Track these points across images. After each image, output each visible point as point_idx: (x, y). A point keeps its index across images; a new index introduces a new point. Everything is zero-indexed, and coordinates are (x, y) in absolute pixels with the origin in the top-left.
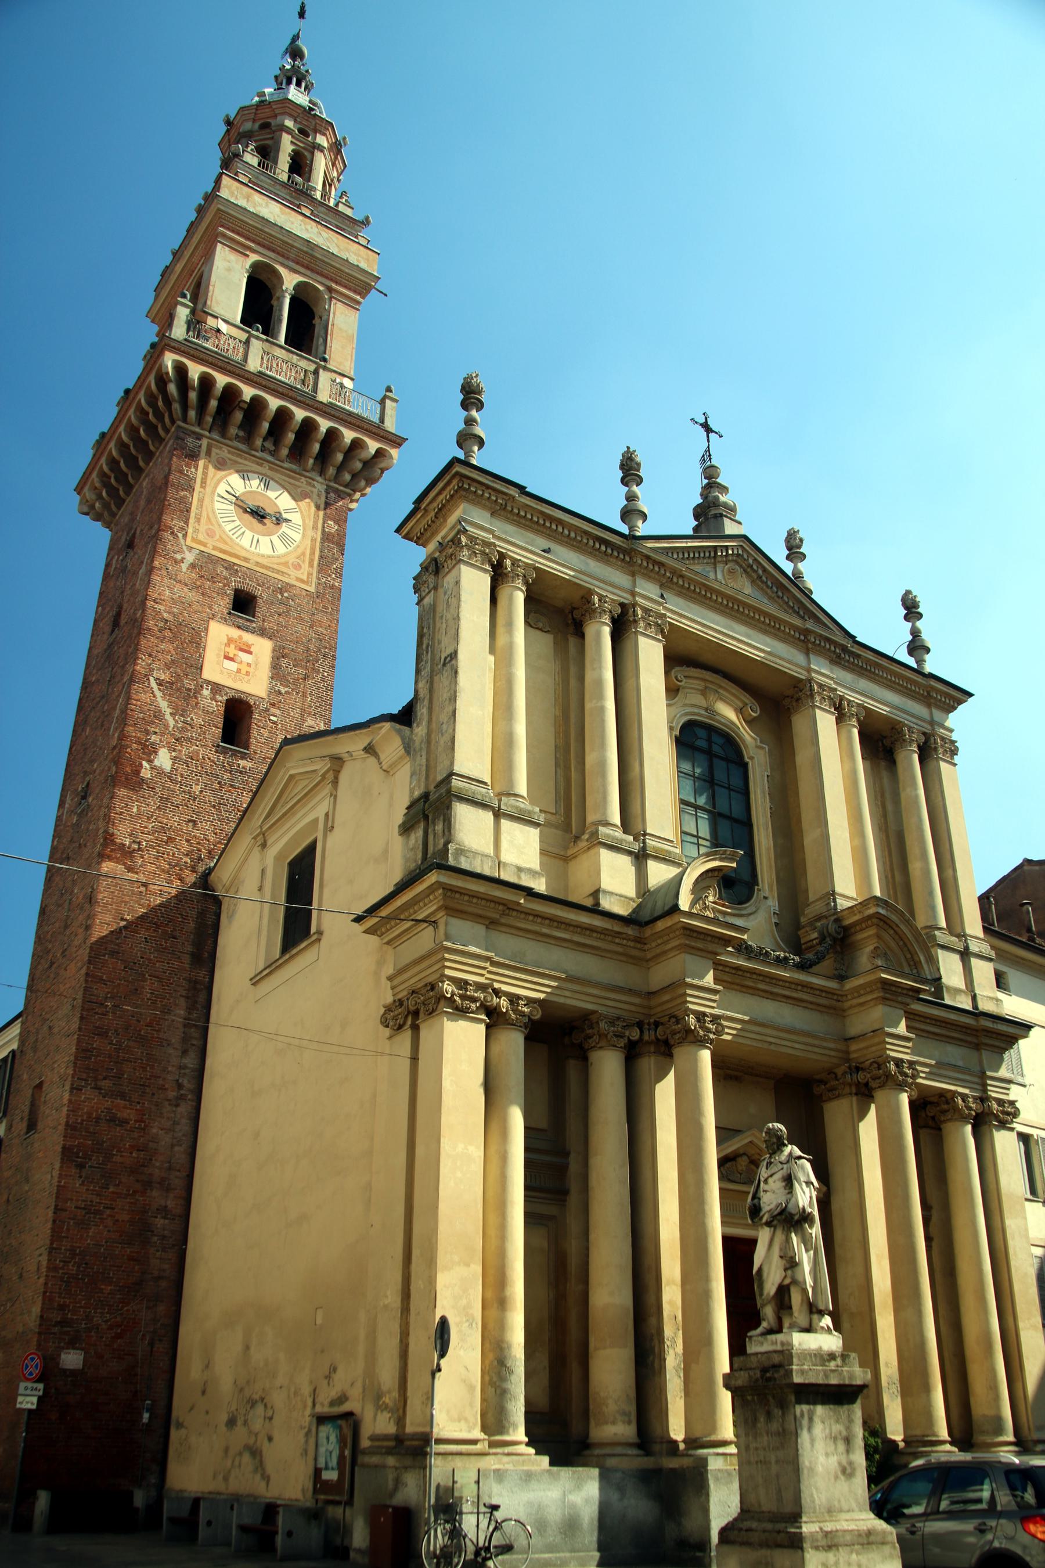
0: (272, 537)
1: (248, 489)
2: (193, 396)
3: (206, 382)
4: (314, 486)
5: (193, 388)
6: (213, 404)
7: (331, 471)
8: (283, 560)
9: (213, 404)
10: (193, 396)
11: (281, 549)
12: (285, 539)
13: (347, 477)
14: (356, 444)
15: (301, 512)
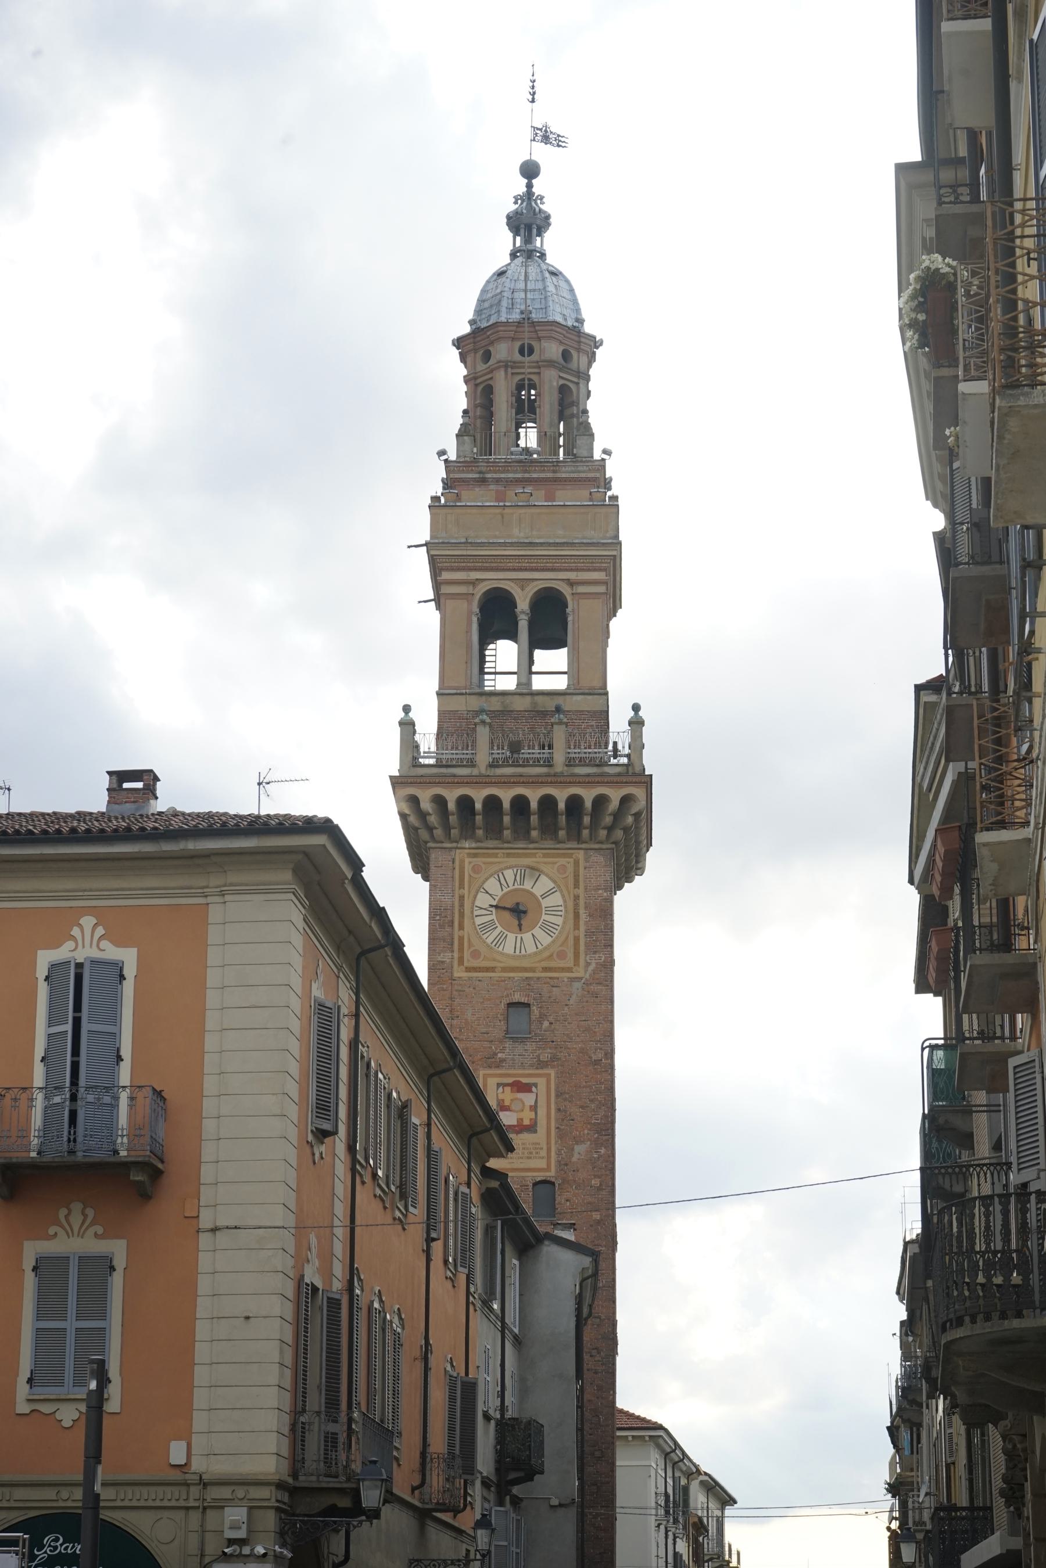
0: (533, 931)
1: (505, 890)
2: (433, 819)
3: (440, 801)
4: (570, 856)
5: (430, 814)
6: (453, 819)
7: (585, 833)
8: (546, 954)
9: (453, 819)
10: (433, 819)
11: (546, 940)
12: (547, 928)
13: (603, 833)
14: (600, 801)
15: (561, 891)
